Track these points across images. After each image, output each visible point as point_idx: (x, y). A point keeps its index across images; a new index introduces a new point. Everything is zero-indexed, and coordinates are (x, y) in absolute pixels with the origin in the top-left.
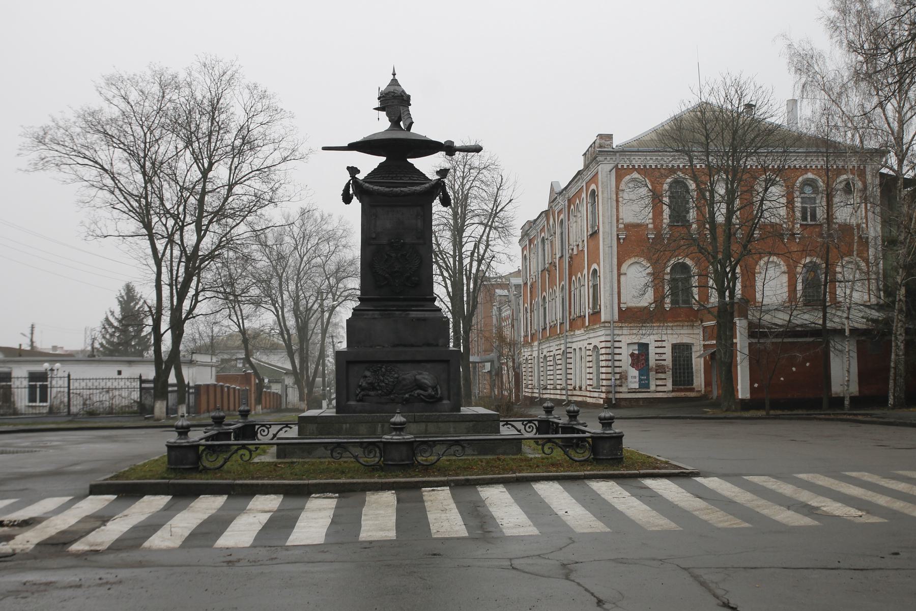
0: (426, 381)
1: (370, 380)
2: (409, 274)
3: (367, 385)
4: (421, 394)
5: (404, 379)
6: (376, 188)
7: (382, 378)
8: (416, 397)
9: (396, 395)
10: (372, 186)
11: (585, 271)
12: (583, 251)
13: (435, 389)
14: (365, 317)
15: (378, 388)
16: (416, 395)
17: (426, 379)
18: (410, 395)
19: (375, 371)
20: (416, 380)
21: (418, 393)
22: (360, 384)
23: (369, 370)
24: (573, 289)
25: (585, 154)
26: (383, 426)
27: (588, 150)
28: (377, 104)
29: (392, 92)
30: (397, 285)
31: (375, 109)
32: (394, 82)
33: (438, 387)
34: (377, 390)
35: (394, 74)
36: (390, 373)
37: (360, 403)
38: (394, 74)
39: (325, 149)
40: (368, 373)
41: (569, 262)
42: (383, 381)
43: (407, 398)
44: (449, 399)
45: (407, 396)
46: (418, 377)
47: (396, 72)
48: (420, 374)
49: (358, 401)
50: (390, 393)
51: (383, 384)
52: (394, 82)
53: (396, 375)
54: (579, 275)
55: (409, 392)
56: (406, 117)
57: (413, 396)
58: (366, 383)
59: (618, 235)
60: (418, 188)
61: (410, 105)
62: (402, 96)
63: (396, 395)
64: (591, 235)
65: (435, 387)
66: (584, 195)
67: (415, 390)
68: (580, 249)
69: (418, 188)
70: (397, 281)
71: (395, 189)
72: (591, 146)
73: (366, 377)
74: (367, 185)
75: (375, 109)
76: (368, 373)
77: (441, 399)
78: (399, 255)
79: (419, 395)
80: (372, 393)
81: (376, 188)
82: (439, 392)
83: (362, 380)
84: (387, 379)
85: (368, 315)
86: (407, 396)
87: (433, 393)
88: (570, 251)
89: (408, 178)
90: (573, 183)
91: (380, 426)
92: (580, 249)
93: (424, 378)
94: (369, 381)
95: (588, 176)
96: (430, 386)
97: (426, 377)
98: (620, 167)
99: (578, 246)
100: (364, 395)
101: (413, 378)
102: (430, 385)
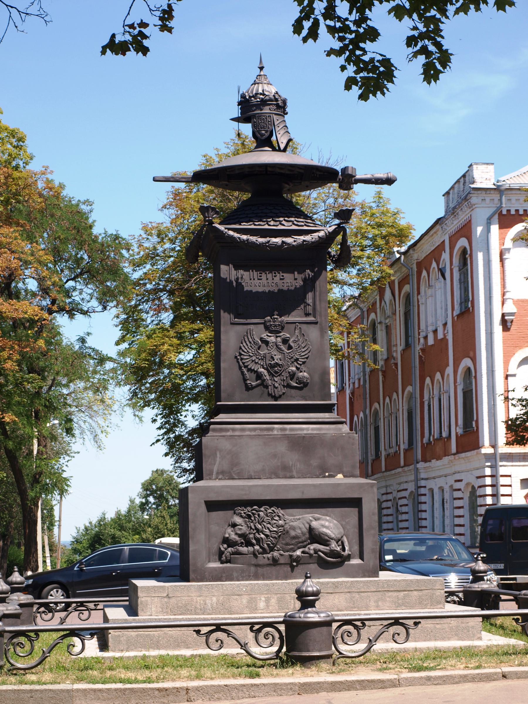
0: (325, 530)
1: (244, 529)
2: (294, 369)
5: (293, 528)
6: (245, 237)
7: (259, 527)
8: (311, 555)
9: (282, 552)
10: (238, 235)
11: (450, 370)
12: (444, 340)
13: (340, 542)
14: (229, 434)
15: (254, 541)
16: (312, 552)
17: (327, 527)
18: (303, 552)
19: (249, 517)
20: (311, 530)
22: (227, 536)
24: (426, 397)
25: (447, 194)
26: (267, 601)
27: (452, 188)
28: (236, 112)
29: (261, 94)
30: (277, 385)
31: (233, 119)
33: (345, 539)
34: (252, 545)
36: (273, 519)
37: (228, 565)
38: (261, 68)
39: (155, 180)
40: (238, 520)
41: (420, 357)
42: (262, 532)
43: (298, 557)
44: (362, 558)
45: (298, 553)
46: (314, 524)
47: (264, 64)
49: (222, 563)
50: (272, 549)
51: (262, 536)
53: (281, 522)
54: (438, 376)
55: (299, 548)
56: (282, 132)
57: (308, 553)
58: (236, 534)
59: (503, 315)
60: (308, 238)
61: (287, 113)
62: (276, 100)
63: (282, 552)
64: (458, 316)
66: (445, 256)
68: (440, 336)
69: (308, 238)
70: (276, 379)
71: (274, 240)
72: (458, 181)
74: (231, 233)
75: (233, 119)
76: (238, 520)
77: (349, 557)
78: (279, 339)
79: (316, 551)
80: (244, 549)
81: (245, 237)
82: (347, 548)
83: (230, 530)
84: (268, 528)
85: (234, 430)
86: (298, 553)
87: (338, 549)
88: (422, 340)
89: (291, 223)
90: (426, 237)
91: (263, 599)
92: (440, 336)
93: (323, 526)
94: (239, 532)
95: (453, 226)
96: (332, 539)
97: (327, 524)
98: (504, 212)
99: (435, 332)
100: (233, 553)
101: (307, 526)
102: (333, 536)
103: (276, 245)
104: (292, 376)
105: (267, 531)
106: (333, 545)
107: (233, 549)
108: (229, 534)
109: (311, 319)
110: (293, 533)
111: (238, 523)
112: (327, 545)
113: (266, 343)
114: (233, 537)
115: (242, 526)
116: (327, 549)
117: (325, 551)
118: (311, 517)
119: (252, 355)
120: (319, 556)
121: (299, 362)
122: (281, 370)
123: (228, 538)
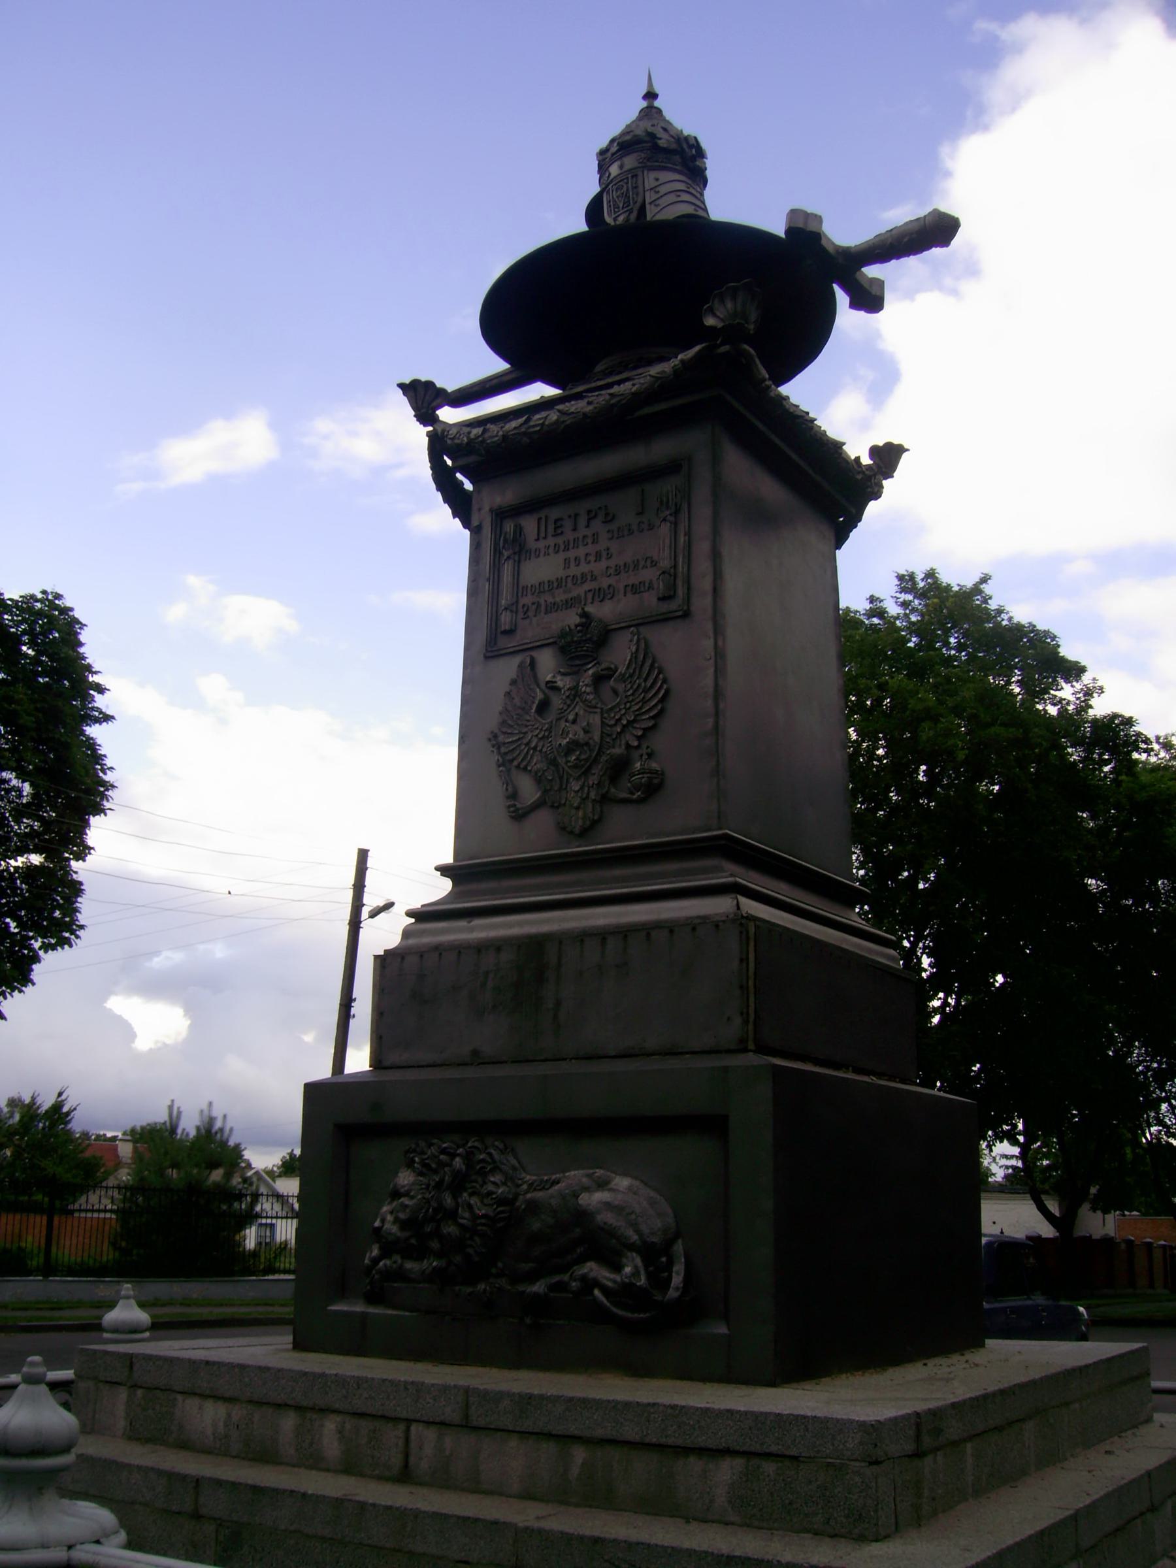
3: (395, 1229)
4: (596, 1283)
5: (534, 1207)
7: (448, 1201)
20: (582, 1216)
21: (584, 1278)
22: (377, 1224)
23: (410, 1164)
32: (651, 112)
33: (679, 1247)
35: (651, 96)
38: (651, 96)
40: (405, 1178)
45: (538, 1287)
47: (657, 89)
48: (602, 1185)
52: (651, 112)
65: (666, 1247)
67: (582, 1260)
73: (396, 1194)
76: (405, 1178)
79: (589, 1284)
82: (677, 1280)
84: (470, 1207)
86: (538, 1287)
96: (632, 1247)
103: (543, 424)
104: (619, 767)
105: (467, 1215)
106: (628, 1270)
107: (388, 1262)
108: (383, 1221)
109: (673, 605)
110: (536, 1225)
111: (402, 1190)
112: (617, 1268)
113: (558, 689)
114: (391, 1227)
115: (412, 1198)
116: (615, 1281)
117: (610, 1284)
118: (588, 1176)
119: (525, 730)
120: (595, 1299)
121: (635, 732)
122: (586, 760)
123: (379, 1229)
